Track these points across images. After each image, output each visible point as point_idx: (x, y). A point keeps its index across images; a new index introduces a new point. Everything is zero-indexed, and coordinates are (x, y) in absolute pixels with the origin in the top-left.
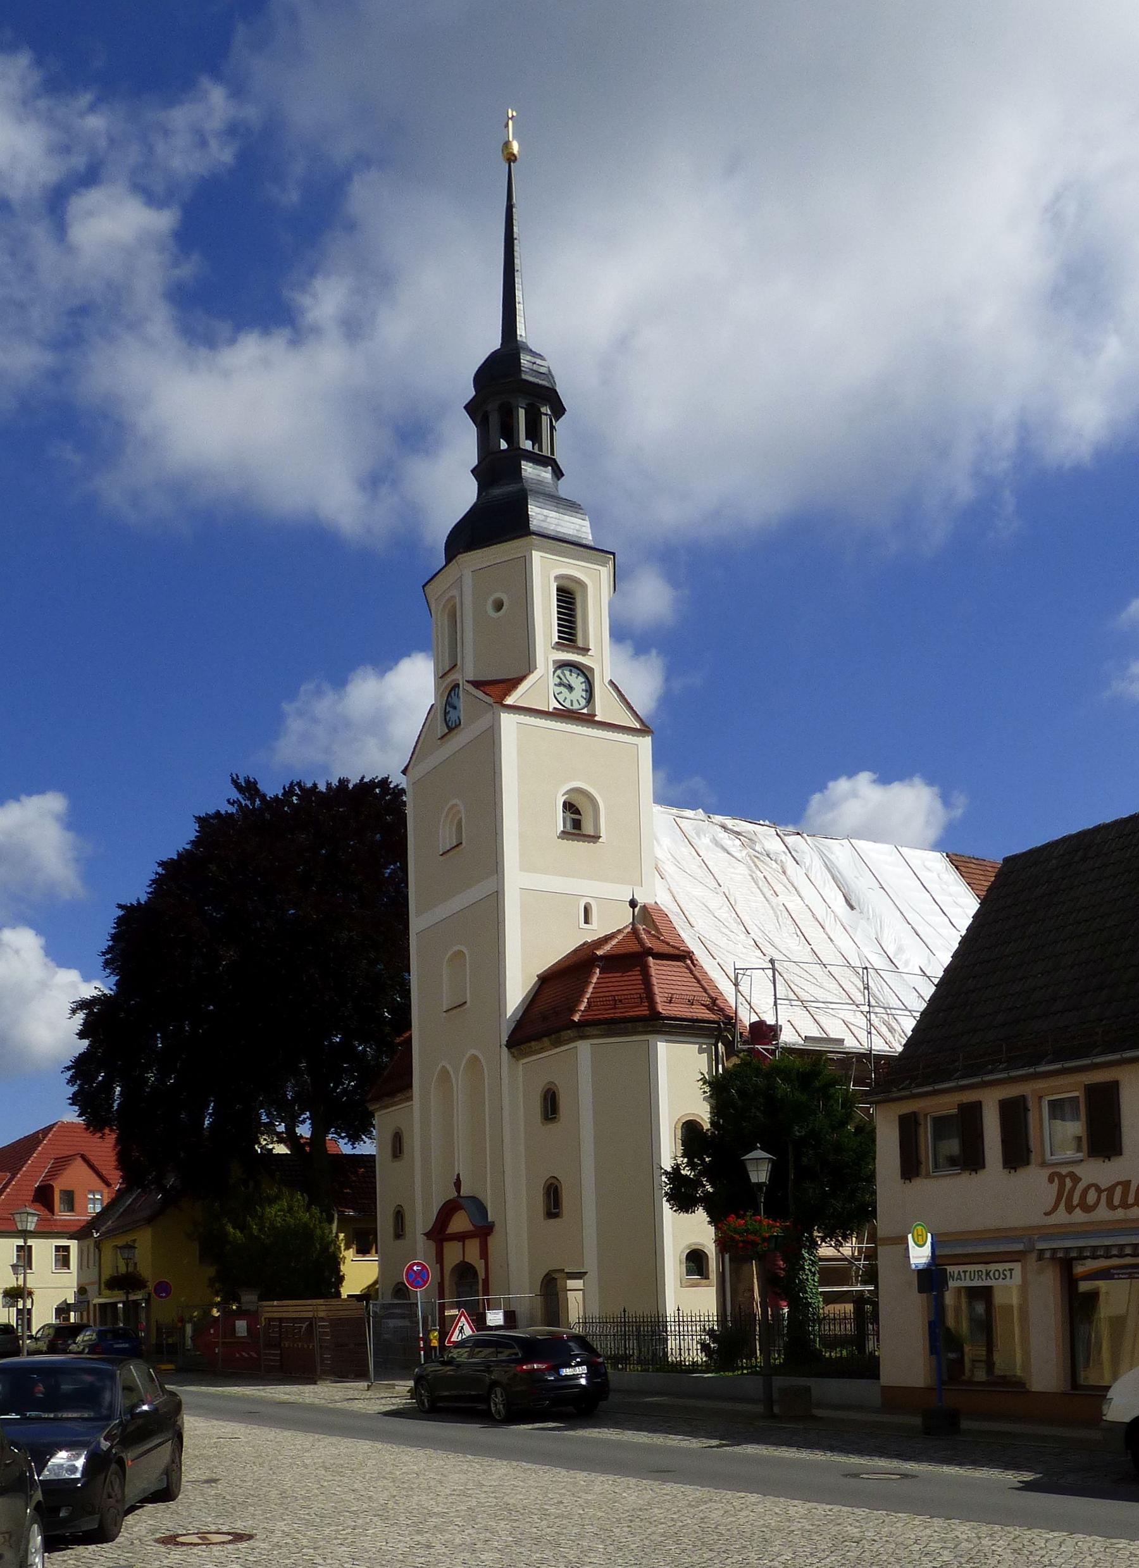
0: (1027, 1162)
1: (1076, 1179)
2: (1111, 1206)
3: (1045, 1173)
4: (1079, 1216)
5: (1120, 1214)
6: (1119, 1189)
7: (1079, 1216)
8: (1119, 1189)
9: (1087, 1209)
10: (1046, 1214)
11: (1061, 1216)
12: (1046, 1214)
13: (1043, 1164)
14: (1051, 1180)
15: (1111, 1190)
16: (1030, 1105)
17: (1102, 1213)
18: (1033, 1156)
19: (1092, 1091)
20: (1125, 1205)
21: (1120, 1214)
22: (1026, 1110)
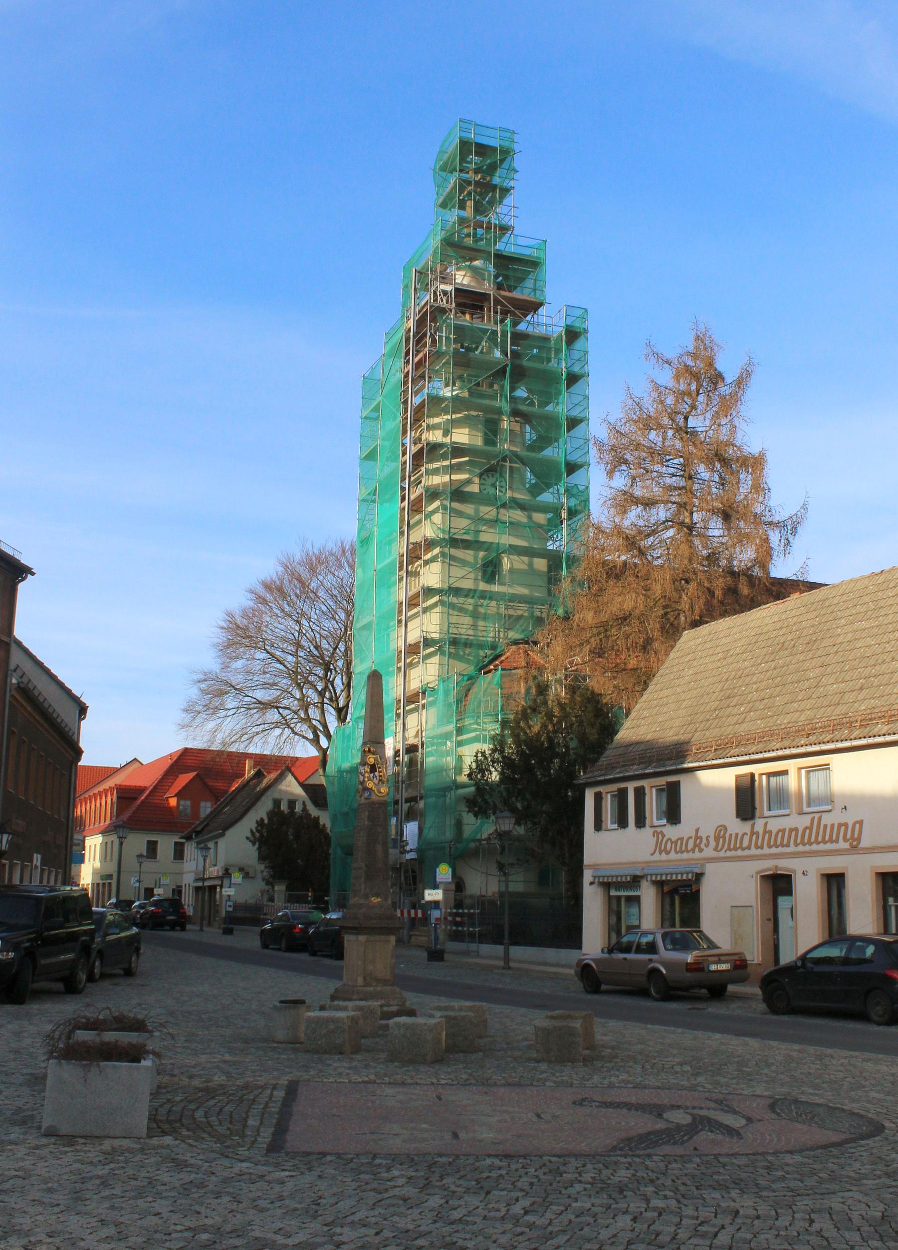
0: (644, 826)
1: (664, 836)
2: (677, 852)
3: (653, 830)
4: (664, 857)
5: (679, 856)
6: (679, 842)
7: (664, 857)
8: (679, 842)
9: (668, 853)
10: (652, 855)
11: (657, 857)
12: (652, 855)
13: (652, 827)
14: (654, 836)
15: (676, 842)
16: (647, 791)
17: (673, 856)
18: (647, 821)
19: (669, 784)
20: (682, 852)
21: (679, 856)
22: (644, 794)
